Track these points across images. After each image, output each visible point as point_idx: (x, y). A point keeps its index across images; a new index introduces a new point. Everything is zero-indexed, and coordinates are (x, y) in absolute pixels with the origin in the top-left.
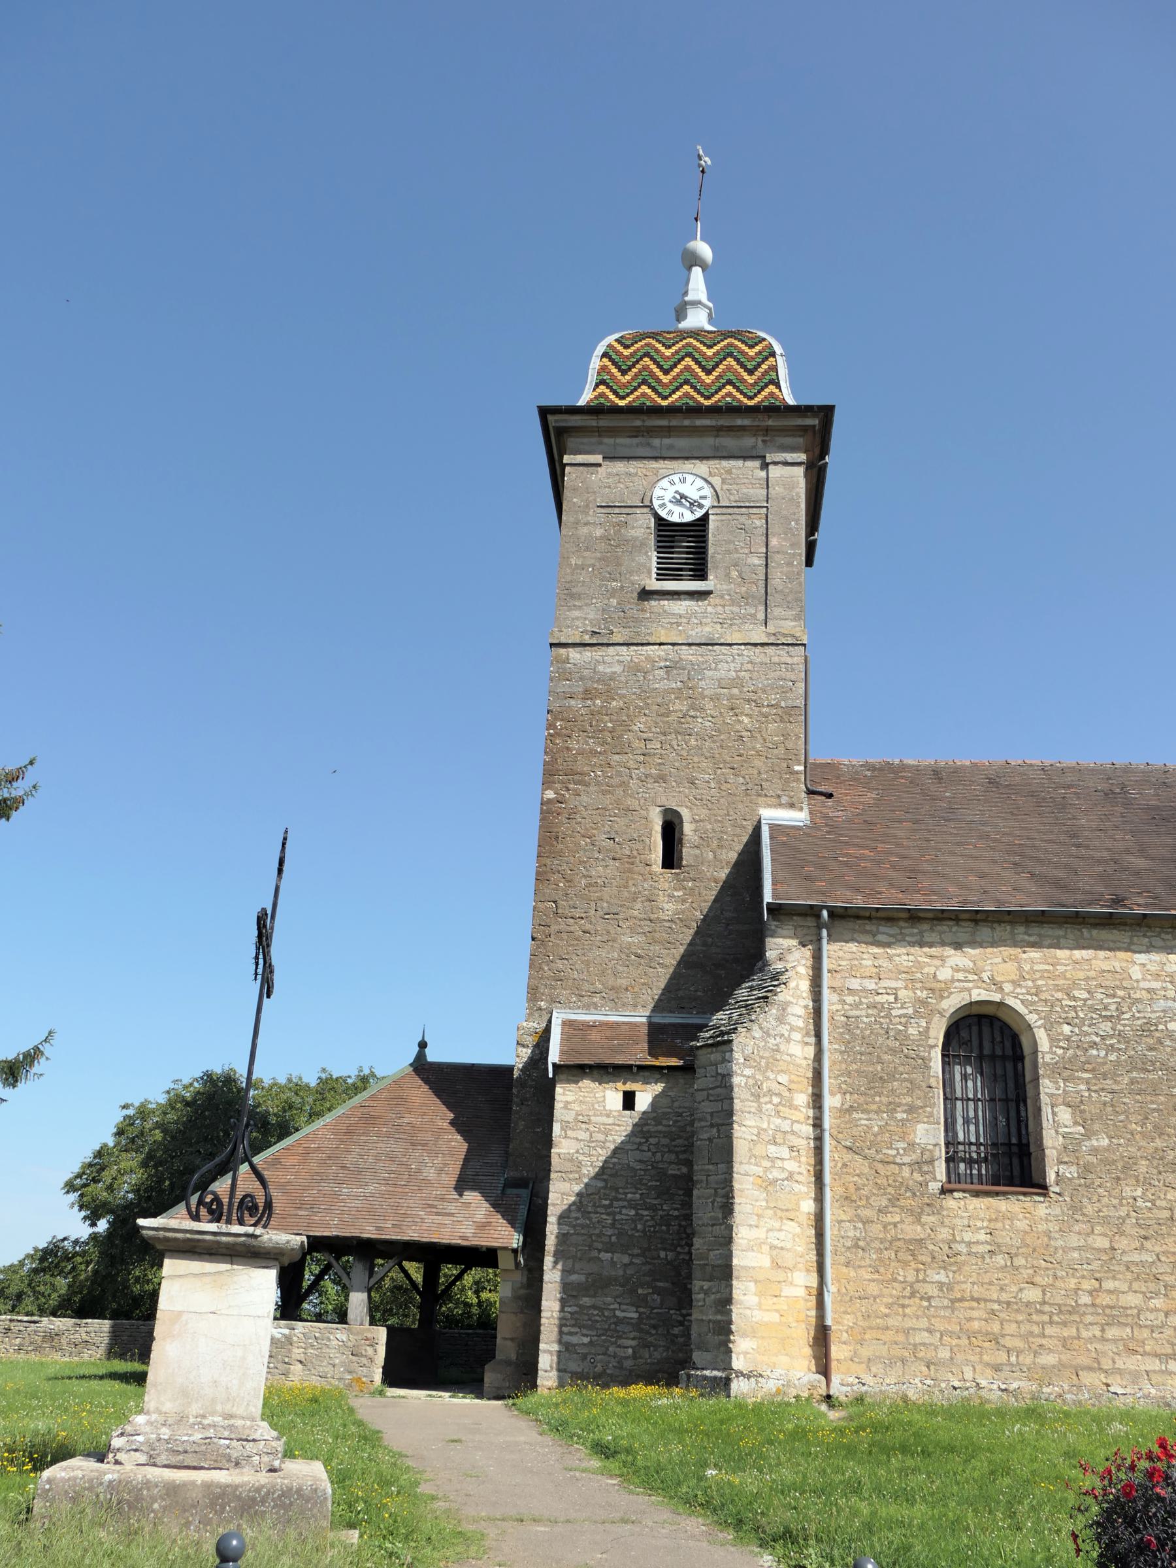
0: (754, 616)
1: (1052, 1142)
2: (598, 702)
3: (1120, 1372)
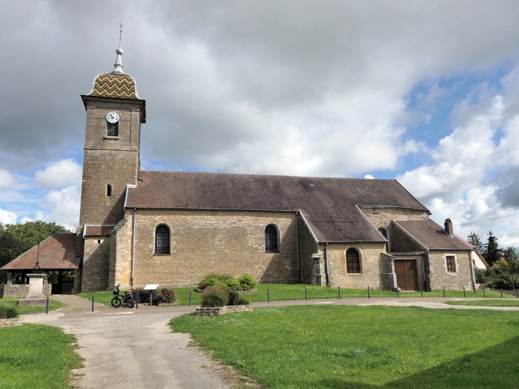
0: (127, 144)
1: (172, 247)
2: (94, 162)
3: (179, 282)
